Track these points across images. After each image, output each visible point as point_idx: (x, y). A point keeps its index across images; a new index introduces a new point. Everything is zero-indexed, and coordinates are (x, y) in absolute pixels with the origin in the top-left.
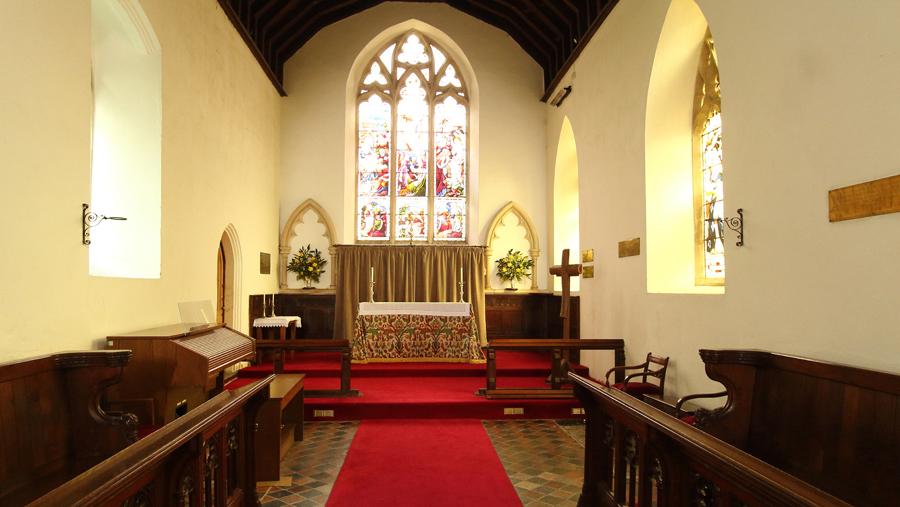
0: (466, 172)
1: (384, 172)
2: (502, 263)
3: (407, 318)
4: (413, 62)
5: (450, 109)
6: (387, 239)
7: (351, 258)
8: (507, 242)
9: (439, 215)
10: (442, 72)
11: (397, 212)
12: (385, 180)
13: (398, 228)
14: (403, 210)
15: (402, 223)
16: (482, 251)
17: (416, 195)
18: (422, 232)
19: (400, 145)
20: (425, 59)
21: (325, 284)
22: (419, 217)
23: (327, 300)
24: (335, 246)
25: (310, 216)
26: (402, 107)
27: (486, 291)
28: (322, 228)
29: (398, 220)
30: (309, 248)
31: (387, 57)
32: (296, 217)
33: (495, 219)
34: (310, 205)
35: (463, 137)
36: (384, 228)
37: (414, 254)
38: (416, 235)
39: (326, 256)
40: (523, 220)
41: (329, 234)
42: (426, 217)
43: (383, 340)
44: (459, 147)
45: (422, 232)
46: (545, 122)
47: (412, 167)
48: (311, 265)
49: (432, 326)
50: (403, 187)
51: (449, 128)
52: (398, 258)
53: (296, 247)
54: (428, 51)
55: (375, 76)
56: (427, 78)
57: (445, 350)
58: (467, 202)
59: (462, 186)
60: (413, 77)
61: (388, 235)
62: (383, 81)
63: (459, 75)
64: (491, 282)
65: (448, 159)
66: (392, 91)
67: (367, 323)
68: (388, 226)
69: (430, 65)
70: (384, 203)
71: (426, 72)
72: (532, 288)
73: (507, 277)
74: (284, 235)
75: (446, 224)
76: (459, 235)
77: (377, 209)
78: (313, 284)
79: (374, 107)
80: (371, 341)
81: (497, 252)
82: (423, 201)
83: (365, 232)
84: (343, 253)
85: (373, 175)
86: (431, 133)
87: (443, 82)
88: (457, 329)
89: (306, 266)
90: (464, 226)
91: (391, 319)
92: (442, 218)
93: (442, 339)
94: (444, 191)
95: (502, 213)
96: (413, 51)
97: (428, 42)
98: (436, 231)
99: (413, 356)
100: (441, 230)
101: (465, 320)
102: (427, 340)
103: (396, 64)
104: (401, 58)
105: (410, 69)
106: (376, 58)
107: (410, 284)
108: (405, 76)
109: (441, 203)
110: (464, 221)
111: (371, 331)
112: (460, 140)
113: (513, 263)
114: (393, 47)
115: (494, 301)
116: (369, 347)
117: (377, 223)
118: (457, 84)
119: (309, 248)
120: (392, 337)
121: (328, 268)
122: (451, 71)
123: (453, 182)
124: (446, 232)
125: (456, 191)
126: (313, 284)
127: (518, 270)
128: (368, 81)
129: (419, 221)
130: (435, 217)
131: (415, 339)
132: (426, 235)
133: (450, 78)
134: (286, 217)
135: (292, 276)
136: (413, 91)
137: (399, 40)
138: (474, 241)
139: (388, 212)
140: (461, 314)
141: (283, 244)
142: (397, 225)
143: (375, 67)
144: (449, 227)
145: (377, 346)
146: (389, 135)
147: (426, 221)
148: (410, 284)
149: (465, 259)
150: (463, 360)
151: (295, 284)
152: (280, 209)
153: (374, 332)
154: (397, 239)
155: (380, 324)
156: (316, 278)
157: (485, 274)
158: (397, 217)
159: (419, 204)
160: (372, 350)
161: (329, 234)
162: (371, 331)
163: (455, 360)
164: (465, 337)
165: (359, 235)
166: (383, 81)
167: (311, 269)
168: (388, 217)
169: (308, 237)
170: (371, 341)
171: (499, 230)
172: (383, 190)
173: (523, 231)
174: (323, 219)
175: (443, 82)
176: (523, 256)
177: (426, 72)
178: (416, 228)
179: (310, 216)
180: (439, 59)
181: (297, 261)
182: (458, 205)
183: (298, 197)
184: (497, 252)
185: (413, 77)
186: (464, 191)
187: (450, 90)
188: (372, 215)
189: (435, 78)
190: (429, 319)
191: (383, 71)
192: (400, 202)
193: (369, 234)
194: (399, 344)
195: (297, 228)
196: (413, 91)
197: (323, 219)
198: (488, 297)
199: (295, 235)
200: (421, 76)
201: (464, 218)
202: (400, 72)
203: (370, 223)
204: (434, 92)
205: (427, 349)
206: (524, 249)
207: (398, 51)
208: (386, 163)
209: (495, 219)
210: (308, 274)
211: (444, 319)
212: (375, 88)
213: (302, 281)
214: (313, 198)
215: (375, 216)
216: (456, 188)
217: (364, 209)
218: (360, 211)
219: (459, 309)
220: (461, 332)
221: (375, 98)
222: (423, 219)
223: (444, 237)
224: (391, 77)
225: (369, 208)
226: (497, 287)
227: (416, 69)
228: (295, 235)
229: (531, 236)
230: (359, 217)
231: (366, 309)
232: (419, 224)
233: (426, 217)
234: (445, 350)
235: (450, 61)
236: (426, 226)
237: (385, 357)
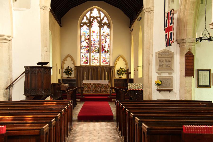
0: (109, 46)
2: (118, 71)
4: (95, 16)
5: (105, 29)
7: (80, 70)
8: (120, 65)
10: (103, 19)
13: (91, 61)
19: (92, 39)
20: (98, 15)
21: (73, 76)
25: (69, 59)
26: (93, 29)
28: (72, 62)
31: (88, 15)
32: (65, 59)
33: (117, 59)
35: (109, 37)
37: (95, 69)
39: (73, 69)
40: (124, 60)
41: (74, 63)
44: (108, 39)
46: (130, 34)
49: (100, 86)
51: (105, 34)
53: (65, 67)
54: (99, 13)
55: (85, 20)
60: (95, 20)
62: (87, 21)
63: (107, 20)
66: (90, 25)
69: (100, 17)
70: (88, 55)
74: (62, 64)
78: (70, 76)
79: (85, 29)
81: (117, 68)
87: (104, 22)
89: (68, 72)
91: (90, 84)
96: (95, 13)
97: (99, 11)
103: (91, 17)
104: (92, 15)
105: (94, 18)
106: (85, 15)
109: (103, 55)
118: (107, 22)
121: (73, 72)
122: (105, 18)
123: (106, 49)
128: (83, 21)
133: (105, 21)
134: (63, 58)
136: (95, 26)
137: (92, 10)
138: (111, 65)
143: (85, 18)
149: (109, 70)
151: (65, 76)
156: (71, 75)
161: (74, 63)
166: (87, 21)
169: (68, 64)
172: (87, 51)
173: (124, 62)
174: (72, 59)
175: (104, 22)
177: (99, 19)
179: (69, 59)
180: (102, 15)
183: (66, 53)
184: (117, 68)
185: (95, 20)
187: (105, 24)
189: (101, 20)
191: (87, 19)
195: (66, 62)
196: (95, 26)
197: (72, 59)
200: (97, 20)
202: (92, 19)
203: (84, 60)
204: (101, 25)
207: (91, 13)
212: (85, 24)
219: (106, 82)
221: (85, 26)
224: (89, 20)
227: (96, 18)
229: (126, 64)
231: (85, 82)
235: (105, 16)
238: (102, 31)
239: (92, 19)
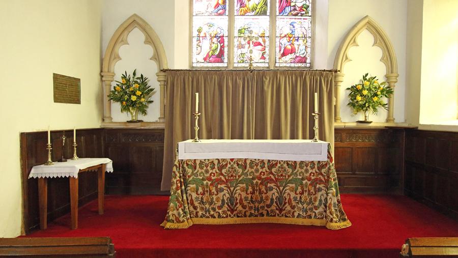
2: (355, 91)
3: (243, 164)
6: (226, 65)
9: (281, 37)
11: (236, 34)
13: (237, 52)
15: (241, 46)
16: (331, 75)
17: (257, 14)
18: (263, 57)
21: (153, 116)
22: (260, 40)
23: (155, 135)
24: (164, 71)
25: (136, 36)
27: (335, 125)
28: (149, 50)
30: (134, 74)
32: (120, 37)
33: (347, 38)
34: (135, 22)
36: (222, 52)
38: (257, 59)
39: (154, 83)
41: (157, 57)
42: (267, 40)
43: (211, 194)
48: (134, 93)
52: (235, 85)
57: (293, 207)
58: (313, 22)
59: (308, 4)
61: (226, 60)
64: (341, 114)
67: (189, 171)
68: (226, 50)
72: (388, 121)
73: (362, 107)
74: (107, 58)
75: (289, 47)
76: (303, 60)
77: (214, 31)
78: (140, 117)
80: (194, 195)
81: (349, 77)
82: (264, 21)
83: (201, 58)
84: (171, 77)
88: (309, 179)
90: (309, 50)
92: (285, 41)
93: (289, 193)
94: (288, 9)
95: (356, 29)
98: (278, 55)
99: (251, 215)
100: (284, 55)
101: (321, 165)
102: (270, 193)
107: (249, 120)
110: (309, 44)
111: (194, 181)
113: (369, 90)
115: (344, 135)
116: (192, 204)
117: (214, 46)
119: (134, 74)
120: (222, 190)
121: (157, 97)
125: (301, 8)
126: (140, 117)
127: (375, 99)
129: (260, 44)
130: (278, 40)
131: (253, 193)
132: (267, 61)
135: (116, 106)
139: (226, 34)
140: (316, 158)
141: (105, 69)
142: (236, 49)
144: (292, 51)
145: (202, 202)
147: (267, 43)
148: (249, 120)
150: (318, 223)
151: (119, 117)
152: (102, 31)
153: (199, 183)
154: (236, 65)
155: (207, 171)
156: (143, 110)
157: (334, 103)
158: (236, 40)
159: (260, 25)
160: (195, 208)
161: (157, 57)
162: (194, 181)
163: (307, 222)
164: (320, 190)
165: (194, 61)
167: (134, 98)
168: (226, 40)
170: (194, 195)
171: (351, 52)
173: (378, 52)
174: (151, 39)
176: (380, 82)
178: (256, 54)
179: (136, 36)
181: (118, 88)
182: (302, 26)
184: (349, 77)
186: (310, 9)
188: (209, 38)
190: (272, 164)
192: (240, 22)
193: (205, 59)
194: (232, 199)
195: (122, 50)
197: (151, 39)
198: (337, 131)
199: (120, 59)
201: (309, 40)
205: (269, 206)
206: (378, 72)
209: (347, 38)
210: (133, 104)
211: (293, 165)
213: (125, 113)
214: (136, 13)
215: (211, 38)
216: (300, 5)
217: (199, 31)
218: (195, 33)
220: (314, 183)
222: (264, 42)
223: (286, 62)
225: (205, 29)
226: (347, 119)
228: (120, 59)
229: (388, 58)
230: (195, 40)
232: (260, 47)
233: (267, 40)
234: (293, 207)
236: (267, 49)
237: (213, 216)
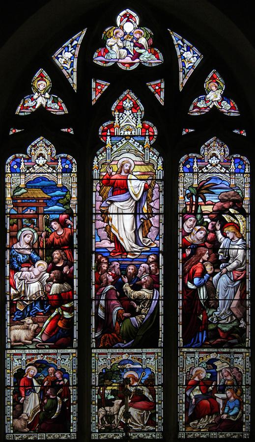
1: (61, 299)
9: (190, 387)
10: (196, 87)
11: (95, 379)
12: (66, 315)
13: (97, 414)
14: (107, 376)
15: (104, 402)
18: (152, 422)
29: (96, 398)
35: (243, 222)
36: (65, 413)
45: (152, 422)
47: (127, 288)
50: (104, 325)
51: (210, 204)
54: (160, 43)
56: (161, 98)
65: (209, 268)
68: (73, 409)
71: (157, 88)
76: (236, 425)
85: (37, 307)
86: (171, 215)
94: (202, 337)
103: (87, 70)
108: (109, 97)
112: (237, 227)
114: (79, 38)
124: (204, 422)
125: (229, 334)
130: (181, 390)
139: (73, 380)
142: (94, 408)
143: (42, 84)
146: (74, 222)
147: (159, 397)
158: (94, 391)
166: (57, 108)
168: (73, 391)
177: (157, 88)
191: (59, 86)
200: (147, 98)
202: (99, 88)
203: (32, 402)
207: (96, 42)
208: (64, 279)
233: (159, 390)
238: (187, 181)
239: (99, 88)
